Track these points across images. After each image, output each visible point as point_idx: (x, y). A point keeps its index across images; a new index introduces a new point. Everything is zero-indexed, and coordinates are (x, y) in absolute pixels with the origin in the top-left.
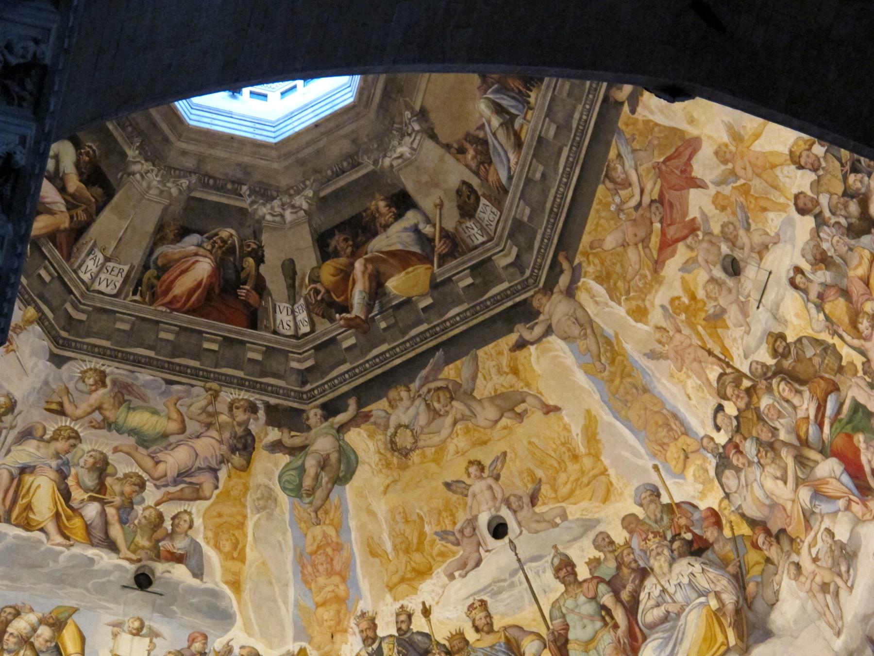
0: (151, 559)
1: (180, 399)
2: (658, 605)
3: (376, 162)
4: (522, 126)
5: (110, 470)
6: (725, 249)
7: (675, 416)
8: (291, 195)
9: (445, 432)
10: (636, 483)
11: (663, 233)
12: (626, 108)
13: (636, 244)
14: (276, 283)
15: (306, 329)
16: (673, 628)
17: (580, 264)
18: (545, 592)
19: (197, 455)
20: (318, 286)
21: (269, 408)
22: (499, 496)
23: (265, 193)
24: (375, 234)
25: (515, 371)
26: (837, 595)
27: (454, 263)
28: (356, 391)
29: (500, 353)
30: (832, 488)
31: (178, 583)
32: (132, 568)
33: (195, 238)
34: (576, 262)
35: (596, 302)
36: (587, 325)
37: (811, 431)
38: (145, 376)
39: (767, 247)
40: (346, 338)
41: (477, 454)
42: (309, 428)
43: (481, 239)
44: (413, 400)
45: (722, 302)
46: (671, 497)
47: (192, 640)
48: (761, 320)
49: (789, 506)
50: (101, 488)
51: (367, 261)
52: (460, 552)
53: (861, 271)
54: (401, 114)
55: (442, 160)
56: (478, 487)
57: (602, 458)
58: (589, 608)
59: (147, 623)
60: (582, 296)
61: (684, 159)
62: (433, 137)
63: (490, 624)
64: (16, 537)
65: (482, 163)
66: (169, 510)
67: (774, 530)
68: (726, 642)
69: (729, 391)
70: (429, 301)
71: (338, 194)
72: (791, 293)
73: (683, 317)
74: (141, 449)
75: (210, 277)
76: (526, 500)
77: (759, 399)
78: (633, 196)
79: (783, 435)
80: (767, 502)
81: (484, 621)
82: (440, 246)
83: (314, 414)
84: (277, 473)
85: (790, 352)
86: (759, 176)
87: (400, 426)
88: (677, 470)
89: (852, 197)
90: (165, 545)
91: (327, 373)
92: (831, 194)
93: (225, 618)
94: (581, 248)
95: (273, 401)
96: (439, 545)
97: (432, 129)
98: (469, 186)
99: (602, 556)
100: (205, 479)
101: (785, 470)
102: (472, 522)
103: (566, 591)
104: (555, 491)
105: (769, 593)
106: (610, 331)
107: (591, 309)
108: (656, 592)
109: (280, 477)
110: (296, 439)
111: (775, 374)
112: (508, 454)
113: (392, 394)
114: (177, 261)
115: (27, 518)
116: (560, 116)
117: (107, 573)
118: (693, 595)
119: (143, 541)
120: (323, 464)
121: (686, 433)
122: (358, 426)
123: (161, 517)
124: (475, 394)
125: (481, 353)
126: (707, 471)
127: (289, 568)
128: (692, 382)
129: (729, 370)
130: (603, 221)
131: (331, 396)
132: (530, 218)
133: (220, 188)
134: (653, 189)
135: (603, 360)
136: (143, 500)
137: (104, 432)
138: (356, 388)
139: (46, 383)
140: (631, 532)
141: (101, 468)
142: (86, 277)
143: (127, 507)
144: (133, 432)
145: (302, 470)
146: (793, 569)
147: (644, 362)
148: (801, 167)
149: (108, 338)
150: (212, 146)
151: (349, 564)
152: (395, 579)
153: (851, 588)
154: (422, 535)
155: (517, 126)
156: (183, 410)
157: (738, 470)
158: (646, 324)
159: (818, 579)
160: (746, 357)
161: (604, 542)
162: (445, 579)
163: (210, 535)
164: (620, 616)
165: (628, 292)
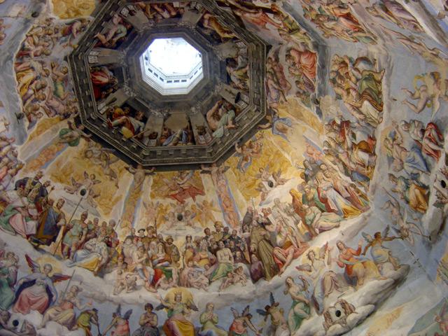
6: (183, 214)
7: (134, 218)
14: (109, 99)
15: (101, 112)
21: (78, 116)
23: (130, 84)
24: (133, 117)
25: (120, 171)
26: (123, 289)
32: (22, 112)
33: (112, 74)
36: (140, 182)
38: (72, 82)
39: (191, 225)
41: (97, 175)
42: (78, 128)
44: (100, 150)
45: (170, 219)
47: (12, 139)
48: (172, 232)
50: (38, 90)
52: (72, 187)
53: (202, 256)
56: (89, 181)
58: (80, 229)
60: (147, 178)
62: (165, 120)
66: (41, 110)
69: (150, 231)
70: (125, 140)
71: (138, 103)
72: (185, 238)
79: (149, 252)
82: (139, 135)
83: (82, 127)
87: (91, 151)
89: (217, 244)
90: (32, 115)
93: (21, 142)
95: (80, 116)
96: (70, 181)
98: (157, 135)
100: (53, 112)
101: (142, 257)
102: (81, 185)
106: (143, 189)
107: (145, 181)
108: (94, 243)
110: (73, 126)
113: (98, 144)
116: (189, 153)
117: (17, 107)
119: (30, 109)
120: (71, 137)
122: (86, 140)
123: (38, 109)
124: (110, 166)
125: (120, 160)
127: (42, 147)
128: (145, 219)
134: (186, 186)
136: (40, 102)
139: (58, 59)
141: (43, 87)
143: (36, 100)
144: (56, 89)
145: (67, 132)
147: (142, 204)
150: (137, 66)
151: (51, 160)
153: (127, 293)
154: (69, 174)
157: (132, 243)
159: (123, 281)
161: (96, 221)
162: (63, 187)
164: (83, 238)
165: (156, 190)
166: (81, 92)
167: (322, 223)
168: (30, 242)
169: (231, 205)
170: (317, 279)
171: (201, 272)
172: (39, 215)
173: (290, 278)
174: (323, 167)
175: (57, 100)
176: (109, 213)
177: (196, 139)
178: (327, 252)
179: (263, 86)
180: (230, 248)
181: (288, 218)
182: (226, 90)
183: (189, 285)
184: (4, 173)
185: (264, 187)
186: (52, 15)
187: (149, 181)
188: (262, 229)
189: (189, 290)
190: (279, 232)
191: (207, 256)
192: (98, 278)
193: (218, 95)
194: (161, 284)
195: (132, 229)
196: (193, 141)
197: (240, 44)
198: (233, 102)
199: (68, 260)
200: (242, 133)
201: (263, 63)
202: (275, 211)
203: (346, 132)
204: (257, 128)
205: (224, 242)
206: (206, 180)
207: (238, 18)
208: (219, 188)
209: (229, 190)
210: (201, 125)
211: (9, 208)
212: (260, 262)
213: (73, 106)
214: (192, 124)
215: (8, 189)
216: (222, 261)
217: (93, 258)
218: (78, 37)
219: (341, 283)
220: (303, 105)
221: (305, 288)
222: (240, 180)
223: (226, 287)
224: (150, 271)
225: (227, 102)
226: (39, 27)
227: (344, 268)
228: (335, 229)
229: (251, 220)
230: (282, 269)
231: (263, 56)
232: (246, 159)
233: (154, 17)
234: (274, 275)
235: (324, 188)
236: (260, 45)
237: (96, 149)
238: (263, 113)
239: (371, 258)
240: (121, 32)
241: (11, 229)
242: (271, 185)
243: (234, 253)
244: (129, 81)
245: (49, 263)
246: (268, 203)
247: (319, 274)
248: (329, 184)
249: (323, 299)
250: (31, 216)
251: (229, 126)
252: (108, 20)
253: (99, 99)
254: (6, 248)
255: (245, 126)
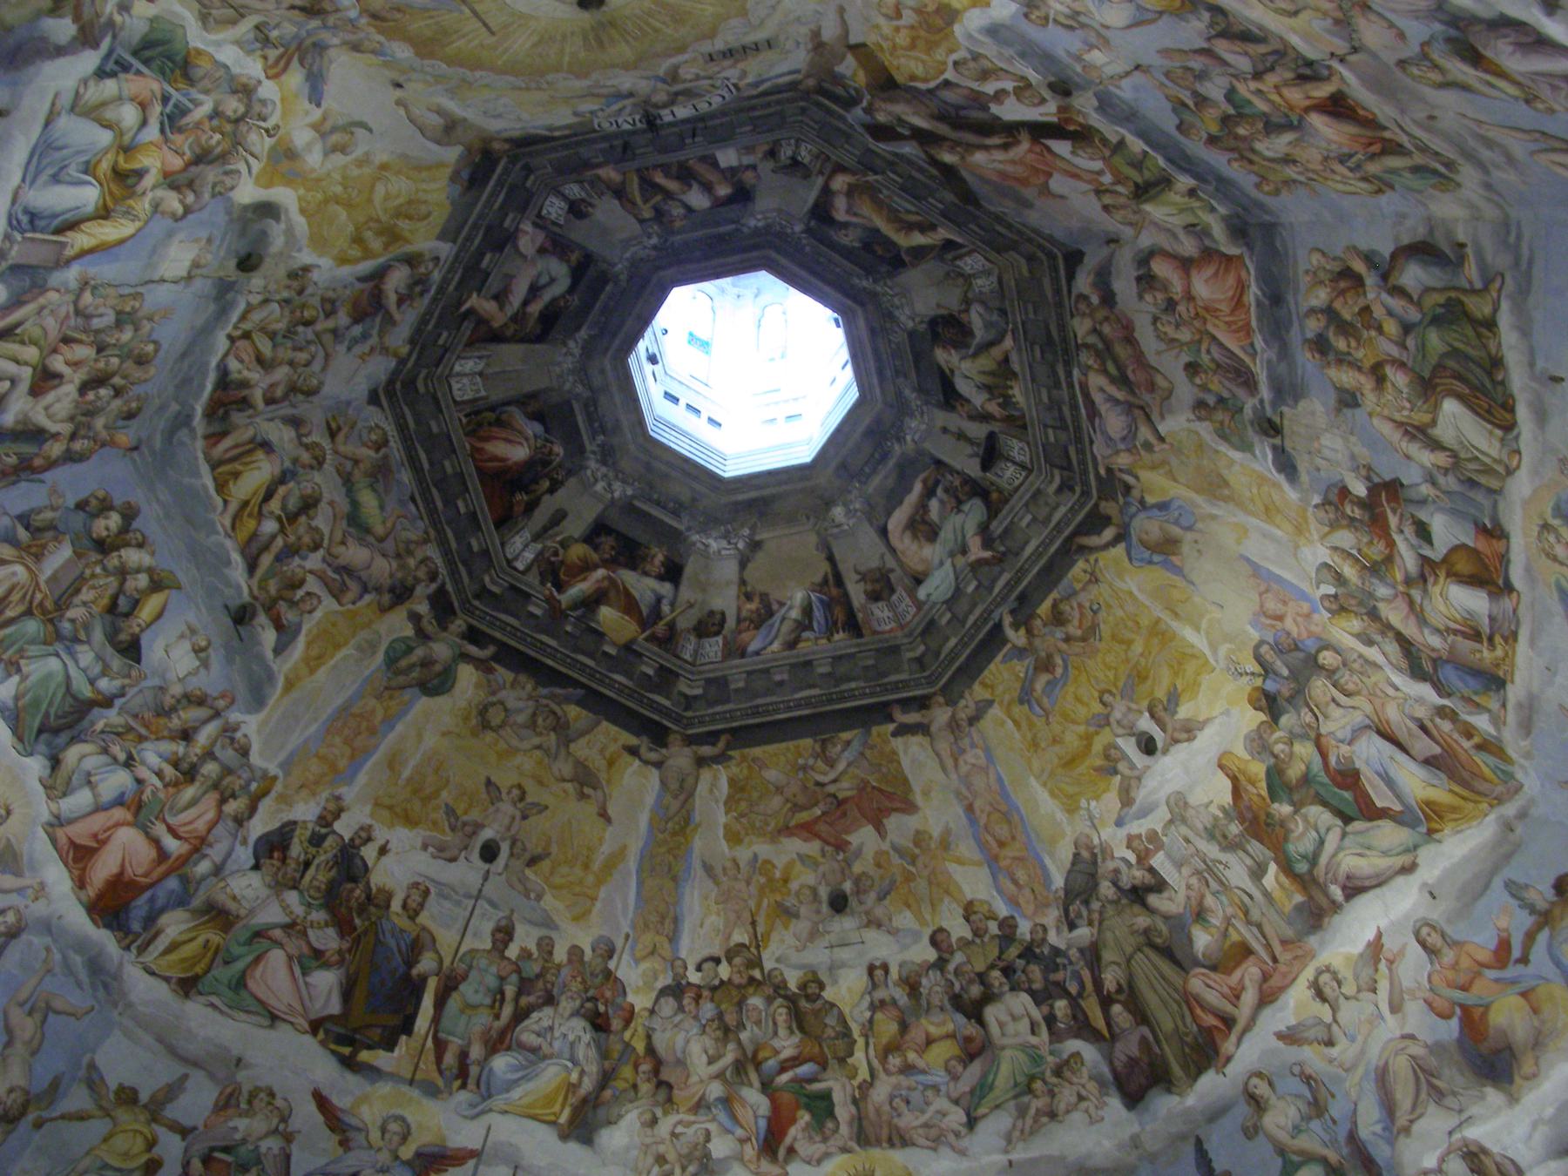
0: (263, 606)
1: (405, 517)
2: (538, 1035)
3: (689, 529)
4: (808, 640)
5: (311, 512)
6: (848, 886)
7: (676, 921)
8: (616, 477)
9: (526, 745)
10: (605, 932)
11: (818, 819)
12: (891, 727)
13: (787, 801)
14: (541, 516)
15: (520, 566)
16: (532, 1063)
17: (730, 758)
18: (475, 935)
19: (369, 567)
20: (561, 551)
21: (442, 591)
22: (513, 831)
23: (607, 455)
24: (634, 568)
27: (656, 649)
28: (502, 645)
29: (615, 740)
30: (745, 1115)
31: (259, 644)
32: (246, 597)
33: (538, 428)
34: (731, 753)
35: (711, 791)
36: (683, 792)
37: (771, 1062)
38: (406, 476)
39: (879, 926)
40: (537, 605)
41: (530, 786)
42: (445, 629)
43: (687, 657)
44: (530, 698)
45: (803, 910)
46: (617, 967)
47: (223, 696)
48: (817, 956)
49: (694, 1079)
50: (293, 518)
51: (609, 578)
52: (449, 837)
53: (932, 1030)
54: (742, 526)
55: (728, 583)
56: (507, 808)
57: (603, 889)
58: (492, 981)
59: (210, 650)
60: (706, 775)
61: (888, 804)
62: (743, 564)
63: (417, 913)
64: (204, 487)
65: (752, 621)
66: (312, 585)
67: (665, 1075)
68: (557, 1115)
69: (737, 961)
70: (612, 651)
73: (763, 880)
74: (344, 523)
75: (516, 464)
76: (527, 856)
77: (754, 994)
78: (825, 774)
79: (744, 1036)
80: (679, 1055)
81: (414, 905)
82: (660, 628)
83: (458, 625)
84: (395, 636)
85: (814, 1001)
86: (930, 883)
87: (501, 703)
88: (638, 955)
89: (982, 983)
90: (282, 606)
91: (498, 610)
92: (969, 961)
93: (258, 700)
94: (747, 751)
95: (449, 587)
96: (440, 815)
97: (748, 560)
99: (536, 954)
100: (354, 587)
102: (478, 827)
103: (489, 952)
104: (552, 873)
105: (615, 1111)
106: (697, 818)
107: (702, 788)
108: (546, 1023)
109: (394, 641)
110: (430, 626)
111: (785, 997)
112: (548, 812)
113: (522, 678)
114: (513, 429)
115: (226, 482)
116: (842, 669)
117: (228, 583)
118: (567, 1055)
119: (273, 587)
120: (426, 663)
121: (671, 940)
122: (477, 668)
123: (302, 582)
124: (572, 746)
125: (605, 724)
126: (656, 979)
127: (329, 711)
129: (753, 950)
130: (782, 758)
131: (484, 628)
132: (737, 690)
133: (590, 418)
134: (845, 789)
135: (670, 825)
136: (304, 558)
137: (339, 481)
138: (505, 644)
139: (349, 403)
140: (570, 961)
141: (309, 504)
142: (457, 368)
143: (290, 551)
144: (355, 504)
146: (648, 1116)
148: (967, 919)
149: (418, 422)
151: (368, 752)
152: (387, 801)
154: (436, 794)
155: (806, 634)
156: (399, 527)
157: (681, 1009)
158: (730, 848)
159: (662, 1149)
160: (778, 960)
161: (546, 946)
162: (419, 844)
163: (315, 631)
164: (507, 1011)
165: (742, 815)
166: (440, 504)
167: (1353, 863)
168: (323, 1043)
169: (1013, 838)
170: (1360, 1071)
171: (935, 1088)
172: (346, 945)
173: (1259, 1075)
174: (1327, 658)
175: (362, 542)
176: (588, 912)
177: (860, 616)
178: (1383, 966)
179: (1073, 397)
180: (1032, 993)
181: (1224, 857)
182: (945, 430)
183: (899, 1139)
184: (211, 815)
185: (1125, 757)
186: (306, 257)
187: (713, 786)
188: (1137, 908)
189: (898, 1156)
190: (1200, 915)
191: (950, 1027)
192: (573, 1147)
193: (921, 452)
194: (797, 1146)
195: (674, 962)
196: (853, 626)
197: (971, 264)
198: (973, 468)
199: (463, 1096)
200: (1022, 572)
201: (1060, 317)
202: (1173, 839)
203: (1393, 521)
204: (1070, 550)
205: (1008, 971)
206: (913, 755)
207: (949, 172)
208: (966, 780)
209: (1000, 780)
210: (874, 563)
211: (240, 932)
212: (1145, 1030)
213: (420, 554)
214: (841, 567)
215: (231, 866)
216: (1005, 1041)
217: (550, 1076)
218: (407, 319)
219: (1452, 1076)
220: (1223, 448)
221: (1317, 1108)
222: (1035, 744)
223: (1031, 1133)
224: (754, 1100)
225: (952, 471)
226: (266, 301)
227: (1454, 1023)
228: (1400, 880)
229: (1093, 879)
230: (1228, 1046)
231: (1058, 292)
232: (1045, 665)
233: (659, 214)
234: (1200, 1071)
235: (1340, 735)
236: (1040, 254)
237: (518, 694)
238: (1086, 493)
239: (1549, 970)
240: (553, 280)
241: (254, 1007)
242: (1148, 746)
243: (1045, 1009)
244: (602, 446)
245: (399, 1112)
246: (1144, 813)
247: (1363, 1052)
248: (1358, 718)
249: (1392, 1142)
250: (318, 954)
251: (972, 557)
252: (500, 248)
253: (505, 521)
254: (241, 1076)
255: (1029, 550)
